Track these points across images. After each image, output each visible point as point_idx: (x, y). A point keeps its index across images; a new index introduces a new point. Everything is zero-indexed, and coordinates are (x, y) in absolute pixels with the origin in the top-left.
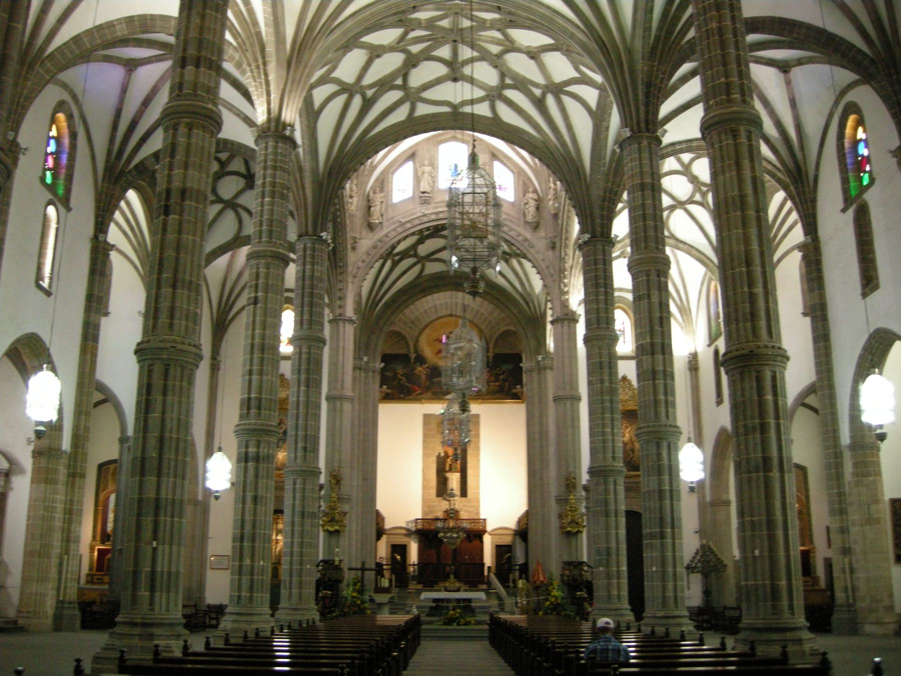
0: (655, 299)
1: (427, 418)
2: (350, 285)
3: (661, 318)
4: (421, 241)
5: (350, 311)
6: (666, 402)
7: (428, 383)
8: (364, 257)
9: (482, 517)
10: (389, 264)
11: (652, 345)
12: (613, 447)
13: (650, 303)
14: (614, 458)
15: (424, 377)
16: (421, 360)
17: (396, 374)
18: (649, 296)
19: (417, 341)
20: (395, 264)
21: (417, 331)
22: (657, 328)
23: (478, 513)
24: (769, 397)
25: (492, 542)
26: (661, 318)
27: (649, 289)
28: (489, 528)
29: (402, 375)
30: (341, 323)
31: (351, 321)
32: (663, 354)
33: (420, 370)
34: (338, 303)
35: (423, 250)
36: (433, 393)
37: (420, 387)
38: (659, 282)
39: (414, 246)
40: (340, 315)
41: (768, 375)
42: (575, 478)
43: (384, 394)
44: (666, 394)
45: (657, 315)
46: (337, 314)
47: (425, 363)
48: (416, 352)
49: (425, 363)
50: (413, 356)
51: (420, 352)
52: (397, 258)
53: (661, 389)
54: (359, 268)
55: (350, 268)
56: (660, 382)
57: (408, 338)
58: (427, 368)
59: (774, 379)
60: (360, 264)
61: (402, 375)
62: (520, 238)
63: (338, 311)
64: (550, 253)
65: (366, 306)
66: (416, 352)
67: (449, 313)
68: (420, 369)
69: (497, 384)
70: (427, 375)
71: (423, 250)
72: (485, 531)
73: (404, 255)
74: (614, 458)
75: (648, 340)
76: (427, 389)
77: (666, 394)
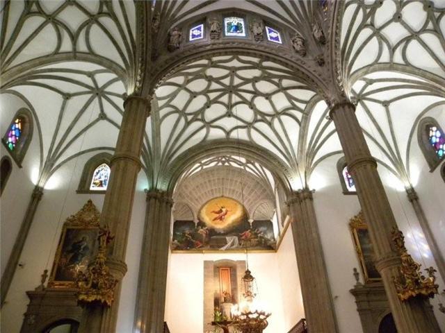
1: (206, 262)
7: (207, 240)
15: (204, 235)
16: (202, 224)
17: (184, 234)
19: (199, 212)
21: (200, 206)
29: (189, 234)
33: (201, 231)
36: (211, 246)
37: (201, 242)
43: (175, 246)
47: (205, 226)
48: (199, 219)
49: (205, 226)
50: (196, 222)
51: (202, 220)
57: (194, 210)
58: (207, 229)
61: (189, 234)
66: (199, 219)
67: (221, 195)
68: (201, 230)
69: (256, 240)
70: (206, 234)
76: (207, 243)
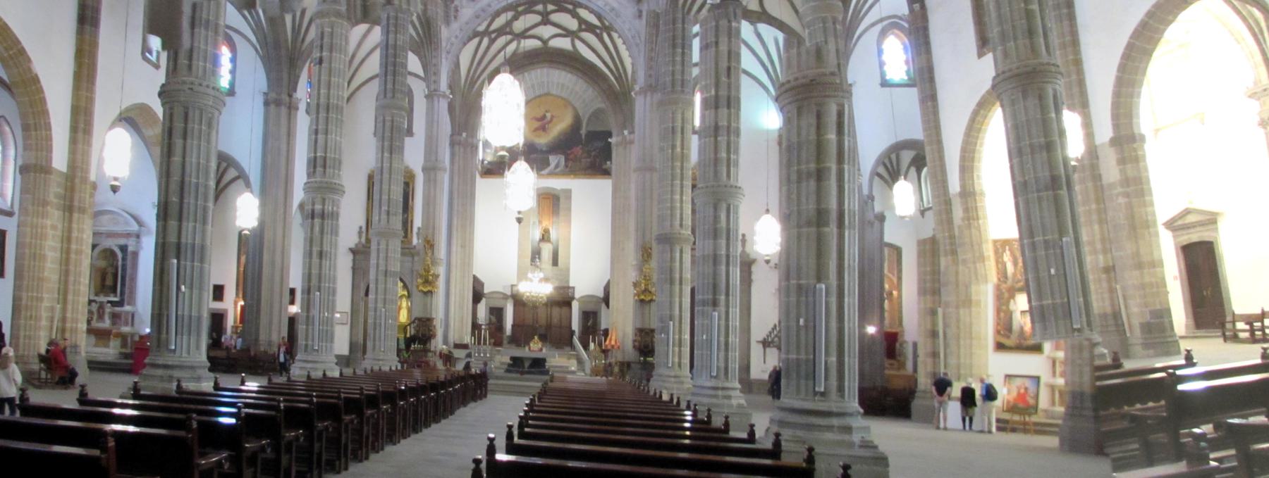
0: (723, 48)
2: (444, 60)
3: (729, 69)
4: (515, 18)
5: (444, 85)
6: (729, 160)
8: (458, 33)
9: (571, 285)
10: (486, 41)
11: (717, 96)
12: (681, 214)
13: (717, 52)
14: (681, 225)
18: (717, 43)
20: (492, 41)
22: (724, 79)
23: (568, 281)
24: (832, 136)
25: (580, 309)
26: (729, 69)
27: (717, 36)
28: (577, 295)
30: (435, 98)
31: (444, 96)
32: (729, 107)
34: (433, 78)
35: (519, 26)
38: (730, 28)
39: (509, 24)
40: (435, 90)
41: (833, 109)
42: (651, 249)
44: (729, 152)
45: (724, 64)
46: (432, 89)
52: (493, 36)
53: (723, 146)
54: (452, 44)
55: (444, 44)
56: (722, 139)
59: (840, 115)
60: (453, 39)
62: (608, 7)
63: (432, 88)
64: (637, 21)
65: (465, 86)
71: (519, 26)
72: (573, 298)
73: (501, 31)
74: (681, 225)
75: (713, 92)
77: (729, 152)
